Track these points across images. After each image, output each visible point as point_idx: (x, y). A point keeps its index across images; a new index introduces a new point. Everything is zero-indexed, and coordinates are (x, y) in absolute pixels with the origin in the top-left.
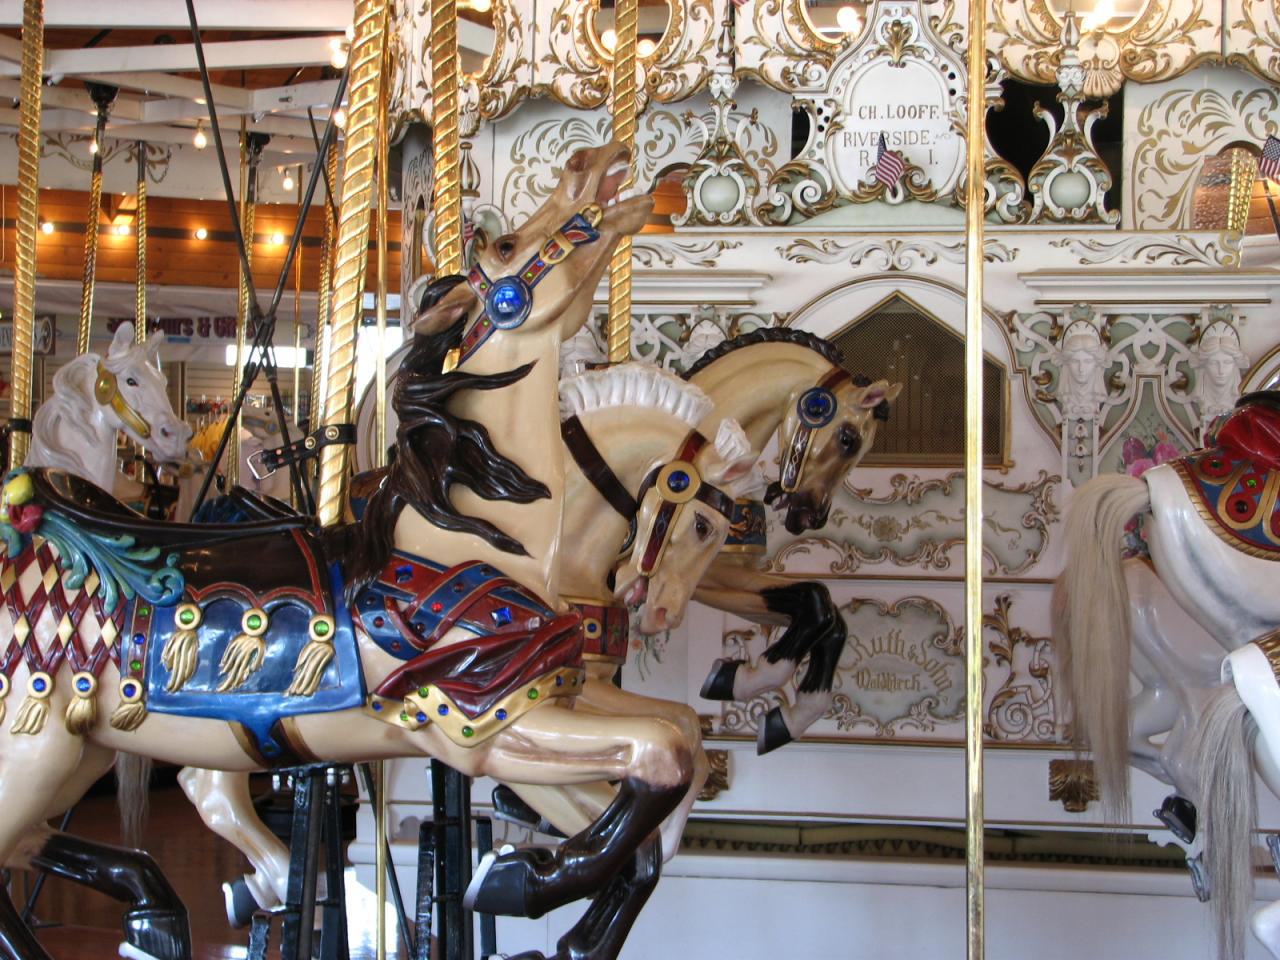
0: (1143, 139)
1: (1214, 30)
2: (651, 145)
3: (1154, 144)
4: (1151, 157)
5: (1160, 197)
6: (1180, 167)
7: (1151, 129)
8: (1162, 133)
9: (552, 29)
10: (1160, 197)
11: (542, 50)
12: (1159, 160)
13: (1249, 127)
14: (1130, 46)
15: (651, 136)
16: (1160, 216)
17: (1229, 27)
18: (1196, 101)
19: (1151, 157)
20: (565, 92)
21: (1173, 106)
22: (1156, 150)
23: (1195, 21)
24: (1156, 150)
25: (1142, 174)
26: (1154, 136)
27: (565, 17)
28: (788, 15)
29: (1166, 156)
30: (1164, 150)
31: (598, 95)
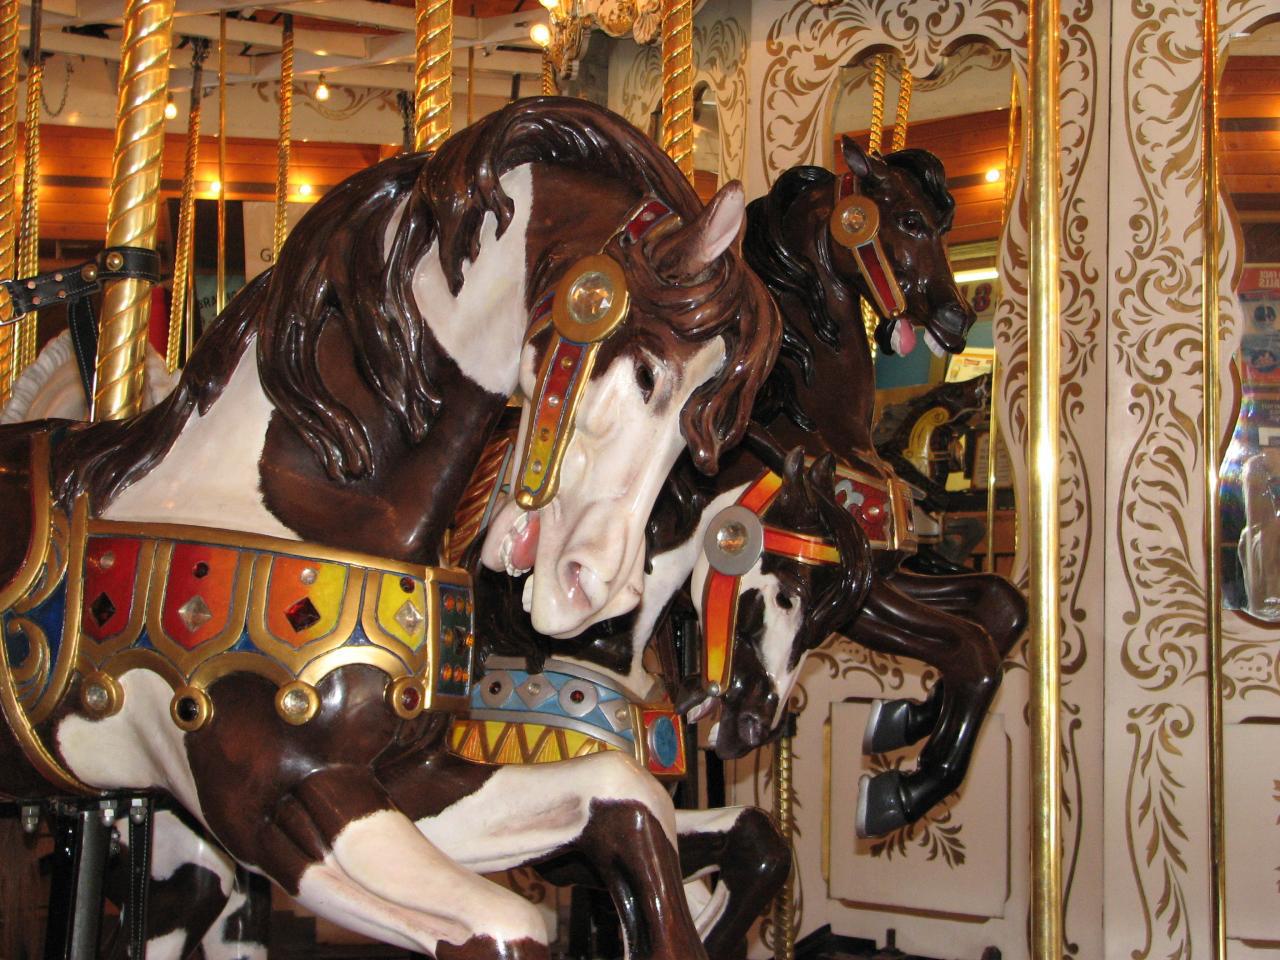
3: (1155, 26)
4: (1151, 44)
5: (1164, 92)
10: (1164, 92)
12: (1163, 45)
25: (1139, 65)
26: (1155, 17)
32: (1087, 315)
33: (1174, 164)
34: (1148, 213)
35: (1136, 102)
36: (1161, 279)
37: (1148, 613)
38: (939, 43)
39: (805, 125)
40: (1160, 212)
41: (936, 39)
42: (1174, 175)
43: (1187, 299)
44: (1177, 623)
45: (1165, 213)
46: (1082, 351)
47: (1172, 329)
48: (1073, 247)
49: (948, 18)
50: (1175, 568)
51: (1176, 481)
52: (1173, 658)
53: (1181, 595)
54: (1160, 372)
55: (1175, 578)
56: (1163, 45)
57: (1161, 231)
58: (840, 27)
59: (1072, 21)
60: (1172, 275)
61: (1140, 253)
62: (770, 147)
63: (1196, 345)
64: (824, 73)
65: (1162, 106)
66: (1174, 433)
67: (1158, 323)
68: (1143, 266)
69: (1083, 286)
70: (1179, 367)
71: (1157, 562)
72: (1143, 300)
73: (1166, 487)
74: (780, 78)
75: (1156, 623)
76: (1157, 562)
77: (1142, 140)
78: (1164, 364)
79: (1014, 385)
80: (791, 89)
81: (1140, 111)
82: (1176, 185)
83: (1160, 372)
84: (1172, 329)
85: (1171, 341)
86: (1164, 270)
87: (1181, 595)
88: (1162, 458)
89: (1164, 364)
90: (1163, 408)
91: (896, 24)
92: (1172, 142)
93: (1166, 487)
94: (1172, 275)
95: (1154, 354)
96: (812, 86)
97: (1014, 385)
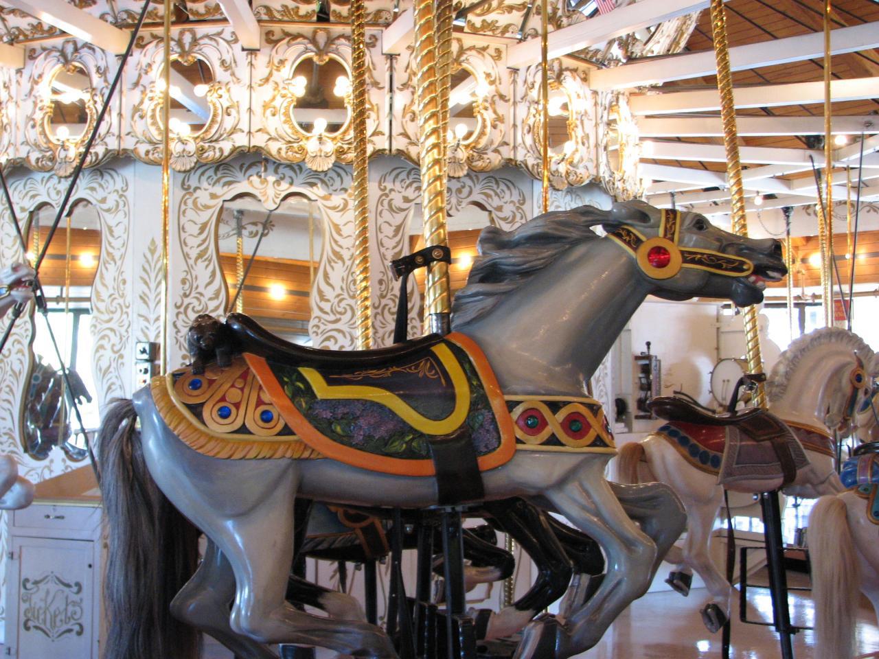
0: (381, 193)
1: (245, 133)
3: (191, 194)
4: (190, 202)
6: (207, 207)
7: (189, 187)
8: (391, 190)
9: (26, 127)
11: (21, 139)
12: (195, 203)
14: (339, 144)
16: (195, 234)
17: (122, 135)
18: (409, 173)
19: (190, 202)
21: (398, 175)
22: (388, 199)
23: (234, 130)
24: (388, 199)
25: (184, 212)
26: (191, 190)
27: (33, 119)
28: (149, 121)
29: (394, 203)
30: (392, 200)
31: (50, 164)
32: (126, 323)
33: (200, 256)
34: (189, 277)
35: (183, 228)
36: (193, 307)
38: (280, 194)
40: (194, 277)
41: (279, 192)
42: (200, 260)
45: (196, 278)
46: (124, 339)
48: (121, 293)
53: (12, 448)
55: (11, 441)
56: (195, 203)
57: (195, 286)
58: (31, 193)
59: (121, 193)
60: (200, 305)
61: (186, 296)
62: (380, 236)
65: (195, 229)
66: (12, 379)
69: (125, 310)
71: (5, 434)
72: (187, 316)
74: (386, 203)
76: (5, 434)
77: (186, 244)
80: (391, 209)
81: (185, 232)
82: (201, 264)
88: (7, 389)
92: (199, 245)
94: (200, 305)
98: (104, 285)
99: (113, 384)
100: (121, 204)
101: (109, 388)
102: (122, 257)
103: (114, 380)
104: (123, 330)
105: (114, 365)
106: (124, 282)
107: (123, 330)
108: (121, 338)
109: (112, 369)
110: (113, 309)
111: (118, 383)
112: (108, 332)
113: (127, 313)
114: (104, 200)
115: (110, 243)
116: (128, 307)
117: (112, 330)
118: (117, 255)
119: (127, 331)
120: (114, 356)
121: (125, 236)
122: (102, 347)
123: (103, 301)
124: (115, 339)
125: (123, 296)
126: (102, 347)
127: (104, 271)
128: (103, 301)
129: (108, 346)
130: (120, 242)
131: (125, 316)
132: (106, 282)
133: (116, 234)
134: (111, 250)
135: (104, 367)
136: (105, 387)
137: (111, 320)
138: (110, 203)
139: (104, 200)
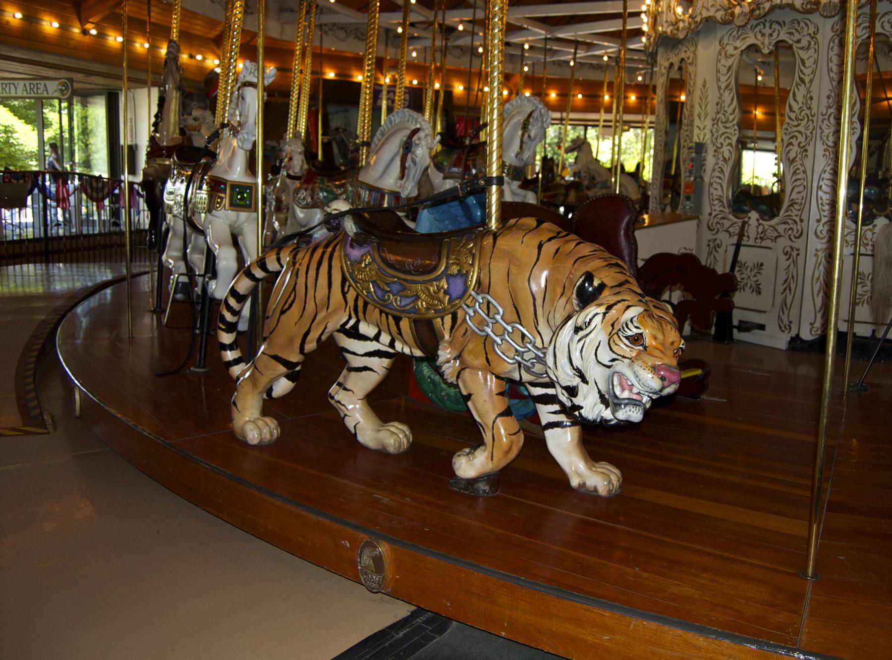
2: (771, 35)
13: (883, 27)
15: (770, 31)
20: (719, 18)
32: (811, 127)
37: (714, 213)
39: (730, 68)
43: (728, 125)
44: (720, 216)
47: (723, 134)
49: (775, 35)
50: (721, 201)
51: (722, 176)
52: (718, 226)
54: (719, 146)
63: (729, 138)
64: (736, 52)
67: (720, 133)
68: (718, 116)
70: (725, 144)
73: (720, 178)
75: (715, 216)
78: (722, 144)
79: (788, 149)
83: (719, 146)
84: (723, 134)
85: (723, 137)
86: (723, 117)
87: (721, 208)
89: (722, 144)
90: (720, 156)
91: (759, 36)
93: (720, 178)
95: (720, 140)
96: (732, 56)
97: (788, 149)
98: (795, 100)
99: (798, 169)
100: (813, 43)
101: (795, 172)
102: (811, 81)
103: (799, 166)
104: (808, 133)
105: (799, 156)
106: (811, 98)
107: (808, 133)
108: (806, 138)
109: (797, 159)
110: (801, 117)
111: (802, 169)
112: (796, 134)
113: (812, 121)
114: (799, 41)
115: (802, 71)
116: (813, 116)
117: (799, 132)
118: (807, 79)
119: (811, 133)
120: (799, 150)
121: (814, 66)
122: (791, 144)
123: (794, 112)
124: (801, 139)
125: (809, 108)
126: (791, 144)
127: (796, 90)
128: (794, 112)
129: (796, 143)
130: (810, 70)
131: (810, 123)
132: (797, 99)
133: (807, 65)
134: (802, 76)
135: (791, 158)
136: (792, 171)
137: (799, 125)
138: (804, 43)
139: (799, 41)
